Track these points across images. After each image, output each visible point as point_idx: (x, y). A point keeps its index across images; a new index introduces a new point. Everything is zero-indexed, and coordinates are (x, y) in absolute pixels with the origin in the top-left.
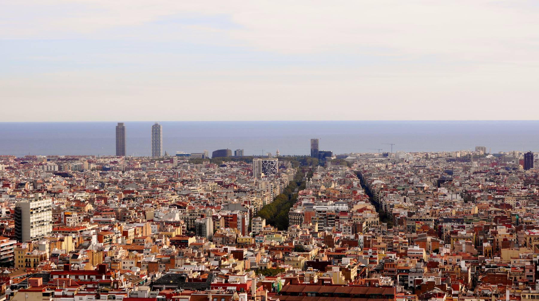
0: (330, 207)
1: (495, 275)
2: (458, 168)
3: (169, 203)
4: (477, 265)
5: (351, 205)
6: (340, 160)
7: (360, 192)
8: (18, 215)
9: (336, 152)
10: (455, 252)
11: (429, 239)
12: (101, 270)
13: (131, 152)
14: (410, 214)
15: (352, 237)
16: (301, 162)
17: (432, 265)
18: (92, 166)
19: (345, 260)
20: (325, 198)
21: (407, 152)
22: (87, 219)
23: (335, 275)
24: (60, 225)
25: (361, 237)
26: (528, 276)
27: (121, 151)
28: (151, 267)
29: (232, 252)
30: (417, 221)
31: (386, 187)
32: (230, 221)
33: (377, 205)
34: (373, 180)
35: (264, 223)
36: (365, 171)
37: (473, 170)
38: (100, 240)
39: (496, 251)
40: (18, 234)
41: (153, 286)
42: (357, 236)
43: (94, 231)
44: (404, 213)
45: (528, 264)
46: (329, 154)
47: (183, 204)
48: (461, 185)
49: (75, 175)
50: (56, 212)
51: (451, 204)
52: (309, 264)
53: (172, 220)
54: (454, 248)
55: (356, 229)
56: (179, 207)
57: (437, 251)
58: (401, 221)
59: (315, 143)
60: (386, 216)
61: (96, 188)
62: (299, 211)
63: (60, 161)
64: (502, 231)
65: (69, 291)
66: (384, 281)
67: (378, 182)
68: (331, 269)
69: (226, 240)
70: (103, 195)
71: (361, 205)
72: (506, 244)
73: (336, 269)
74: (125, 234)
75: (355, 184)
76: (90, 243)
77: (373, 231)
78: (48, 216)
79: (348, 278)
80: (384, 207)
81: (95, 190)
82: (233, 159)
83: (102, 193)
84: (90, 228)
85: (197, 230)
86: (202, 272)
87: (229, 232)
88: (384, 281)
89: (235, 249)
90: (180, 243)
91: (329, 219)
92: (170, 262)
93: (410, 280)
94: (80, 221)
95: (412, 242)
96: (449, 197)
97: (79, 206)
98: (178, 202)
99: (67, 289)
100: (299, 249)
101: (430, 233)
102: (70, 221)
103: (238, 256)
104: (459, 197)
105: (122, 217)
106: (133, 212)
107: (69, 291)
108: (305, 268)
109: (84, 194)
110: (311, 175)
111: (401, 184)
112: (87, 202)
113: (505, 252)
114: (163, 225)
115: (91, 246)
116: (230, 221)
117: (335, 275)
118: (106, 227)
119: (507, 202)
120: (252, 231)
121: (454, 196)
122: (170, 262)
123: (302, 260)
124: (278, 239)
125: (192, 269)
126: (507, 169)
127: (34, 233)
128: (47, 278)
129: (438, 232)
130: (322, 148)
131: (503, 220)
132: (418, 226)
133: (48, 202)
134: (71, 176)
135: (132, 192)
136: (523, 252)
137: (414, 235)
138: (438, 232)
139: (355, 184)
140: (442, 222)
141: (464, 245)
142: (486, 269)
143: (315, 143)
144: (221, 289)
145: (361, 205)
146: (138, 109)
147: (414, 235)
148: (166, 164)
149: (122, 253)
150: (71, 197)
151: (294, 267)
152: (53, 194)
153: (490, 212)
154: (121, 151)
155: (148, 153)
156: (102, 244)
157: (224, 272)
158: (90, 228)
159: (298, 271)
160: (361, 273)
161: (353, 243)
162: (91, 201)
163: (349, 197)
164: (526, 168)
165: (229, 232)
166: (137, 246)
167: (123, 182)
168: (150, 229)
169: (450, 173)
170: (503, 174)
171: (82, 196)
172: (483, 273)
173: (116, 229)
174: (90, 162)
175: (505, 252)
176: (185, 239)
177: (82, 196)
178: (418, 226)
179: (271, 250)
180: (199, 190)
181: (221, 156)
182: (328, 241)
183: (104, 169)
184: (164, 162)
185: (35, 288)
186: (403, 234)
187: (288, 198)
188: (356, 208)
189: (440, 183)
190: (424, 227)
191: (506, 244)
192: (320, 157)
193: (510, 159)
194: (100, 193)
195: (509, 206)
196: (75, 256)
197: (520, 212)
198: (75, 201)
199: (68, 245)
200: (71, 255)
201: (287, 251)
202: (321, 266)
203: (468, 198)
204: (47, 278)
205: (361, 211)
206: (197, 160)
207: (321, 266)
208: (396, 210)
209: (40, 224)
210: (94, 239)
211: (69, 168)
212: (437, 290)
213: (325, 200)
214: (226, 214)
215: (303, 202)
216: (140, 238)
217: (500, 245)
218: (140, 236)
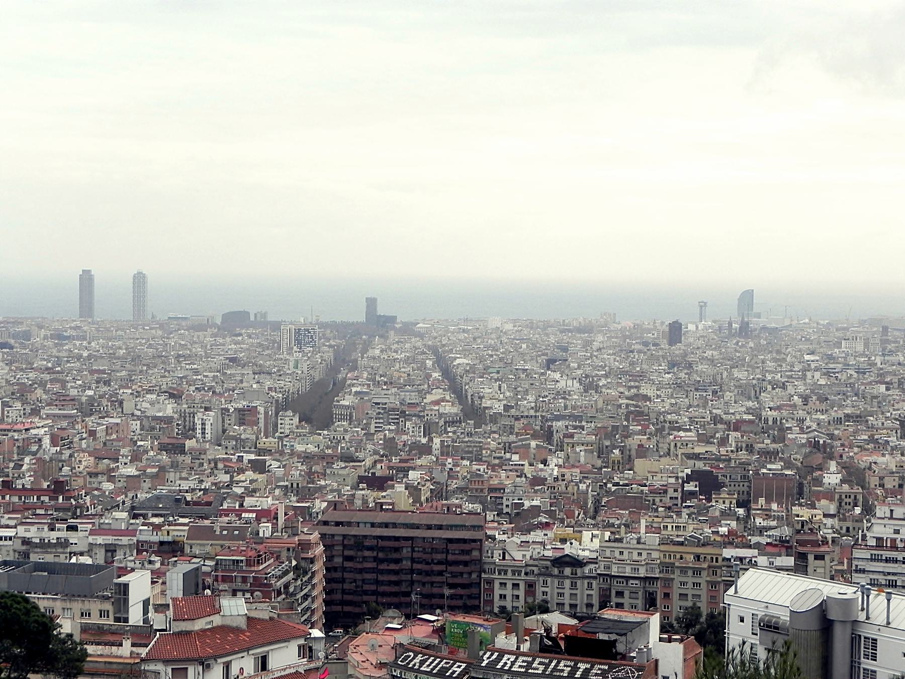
1: (625, 497)
2: (577, 343)
3: (157, 388)
5: (422, 394)
6: (408, 330)
7: (436, 375)
9: (403, 317)
11: (533, 444)
14: (507, 408)
15: (424, 441)
18: (43, 332)
19: (413, 475)
20: (386, 383)
22: (35, 412)
25: (437, 441)
26: (671, 498)
29: (250, 461)
30: (517, 419)
31: (472, 369)
33: (459, 394)
34: (455, 358)
35: (296, 420)
36: (444, 345)
37: (596, 345)
38: (54, 443)
39: (627, 462)
42: (431, 440)
43: (46, 429)
44: (498, 407)
45: (672, 480)
46: (393, 319)
47: (178, 390)
48: (579, 368)
49: (17, 345)
51: (565, 394)
52: (361, 479)
53: (160, 414)
54: (568, 457)
56: (172, 396)
57: (545, 462)
58: (494, 419)
59: (371, 303)
61: (50, 365)
62: (345, 403)
65: (9, 518)
68: (393, 487)
70: (60, 376)
71: (436, 395)
72: (642, 452)
73: (400, 488)
74: (92, 433)
75: (429, 363)
76: (40, 446)
77: (454, 432)
79: (417, 500)
80: (469, 397)
81: (47, 369)
82: (253, 325)
83: (58, 372)
86: (205, 490)
87: (246, 433)
89: (253, 457)
93: (505, 503)
94: (24, 414)
95: (508, 448)
96: (562, 384)
98: (171, 388)
99: (6, 516)
100: (348, 458)
101: (535, 436)
102: (10, 414)
103: (259, 467)
104: (577, 385)
106: (105, 402)
107: (9, 518)
108: (356, 487)
109: (32, 375)
110: (364, 351)
112: (36, 386)
113: (639, 463)
115: (42, 451)
118: (65, 424)
119: (643, 391)
120: (280, 431)
121: (570, 382)
123: (350, 472)
126: (646, 344)
130: (381, 311)
132: (518, 425)
134: (12, 348)
135: (103, 372)
136: (665, 463)
137: (513, 438)
138: (548, 435)
139: (429, 363)
140: (552, 420)
141: (582, 453)
142: (614, 488)
143: (371, 303)
144: (233, 517)
145: (436, 395)
147: (513, 438)
148: (153, 331)
150: (12, 379)
151: (339, 483)
153: (620, 406)
156: (58, 448)
157: (239, 491)
159: (347, 490)
161: (426, 450)
162: (42, 384)
164: (671, 344)
165: (246, 433)
167: (90, 357)
169: (565, 350)
170: (639, 352)
172: (609, 492)
173: (78, 427)
174: (40, 327)
175: (639, 463)
176: (181, 442)
178: (518, 425)
179: (307, 458)
183: (59, 337)
184: (151, 329)
186: (497, 436)
188: (429, 398)
189: (550, 364)
190: (526, 427)
193: (649, 331)
194: (53, 373)
195: (647, 398)
196: (19, 466)
198: (18, 384)
200: (12, 465)
201: (329, 460)
202: (378, 483)
203: (589, 386)
205: (437, 403)
207: (378, 483)
208: (486, 403)
210: (46, 441)
212: (543, 519)
213: (385, 387)
214: (241, 406)
215: (354, 389)
216: (113, 440)
217: (633, 453)
218: (114, 436)
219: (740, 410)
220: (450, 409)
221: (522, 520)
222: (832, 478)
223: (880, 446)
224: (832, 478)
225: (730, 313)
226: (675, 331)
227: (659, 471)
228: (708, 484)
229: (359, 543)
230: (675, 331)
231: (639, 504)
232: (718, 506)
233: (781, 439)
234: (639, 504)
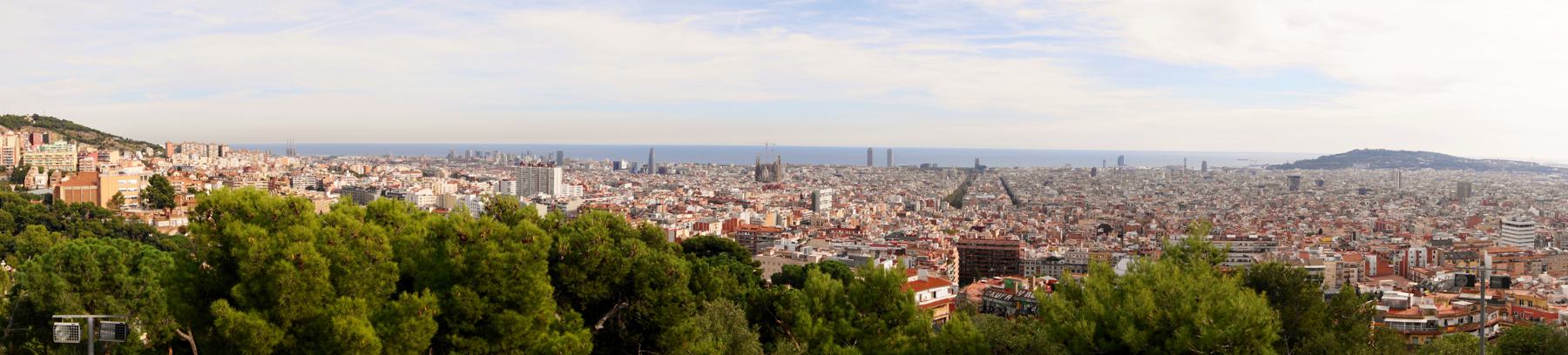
0: (985, 196)
2: (1056, 176)
4: (1066, 230)
6: (991, 170)
8: (814, 197)
9: (989, 166)
10: (1054, 221)
12: (858, 228)
13: (875, 165)
16: (969, 171)
17: (1041, 229)
21: (1028, 167)
23: (987, 234)
24: (836, 203)
27: (870, 163)
28: (886, 228)
32: (930, 204)
33: (1011, 196)
39: (1075, 221)
40: (813, 207)
41: (887, 238)
50: (834, 196)
55: (999, 208)
60: (1015, 202)
63: (837, 169)
64: (1079, 210)
66: (1014, 237)
67: (1011, 183)
69: (927, 214)
72: (1082, 217)
78: (829, 198)
84: (852, 206)
85: (912, 208)
87: (928, 209)
88: (1014, 237)
90: (902, 215)
91: (984, 203)
92: (896, 225)
97: (847, 193)
103: (934, 222)
105: (870, 200)
111: (1025, 183)
114: (893, 205)
116: (930, 204)
117: (987, 234)
122: (896, 225)
124: (957, 213)
125: (908, 230)
127: (822, 207)
128: (828, 232)
129: (1045, 211)
131: (1080, 204)
133: (830, 190)
136: (1091, 221)
138: (1045, 211)
146: (880, 139)
149: (869, 220)
152: (832, 186)
154: (870, 163)
155: (885, 165)
158: (852, 206)
160: (1002, 233)
161: (997, 217)
163: (996, 191)
165: (928, 209)
166: (878, 216)
168: (885, 207)
171: (848, 188)
177: (848, 188)
179: (952, 219)
180: (912, 186)
181: (925, 167)
182: (984, 215)
183: (860, 173)
185: (822, 237)
187: (962, 192)
191: (1082, 217)
192: (980, 168)
197: (1089, 200)
199: (840, 214)
202: (979, 229)
203: (1061, 192)
204: (828, 232)
206: (912, 169)
207: (979, 229)
209: (825, 203)
211: (841, 172)
219: (1119, 202)
220: (1008, 202)
221: (1035, 243)
222: (1153, 226)
223: (1171, 213)
224: (1153, 226)
225: (1114, 164)
226: (1094, 171)
227: (1087, 225)
228: (1107, 229)
229: (972, 251)
230: (1094, 171)
231: (1080, 237)
232: (1111, 237)
233: (1134, 211)
234: (1080, 237)
